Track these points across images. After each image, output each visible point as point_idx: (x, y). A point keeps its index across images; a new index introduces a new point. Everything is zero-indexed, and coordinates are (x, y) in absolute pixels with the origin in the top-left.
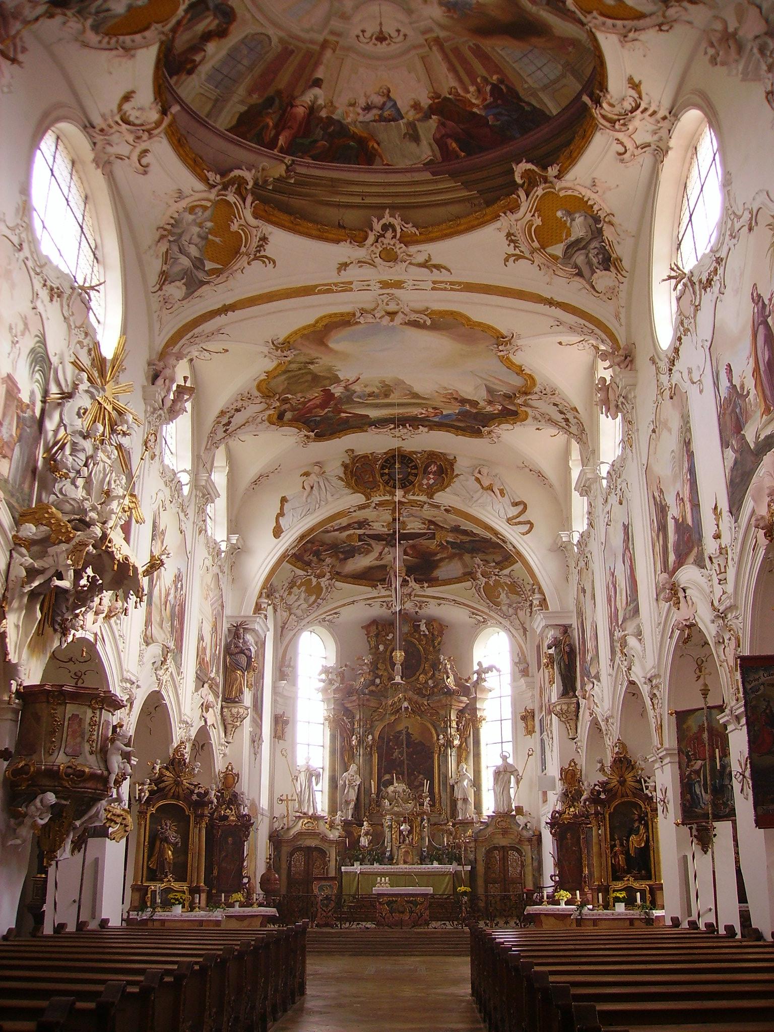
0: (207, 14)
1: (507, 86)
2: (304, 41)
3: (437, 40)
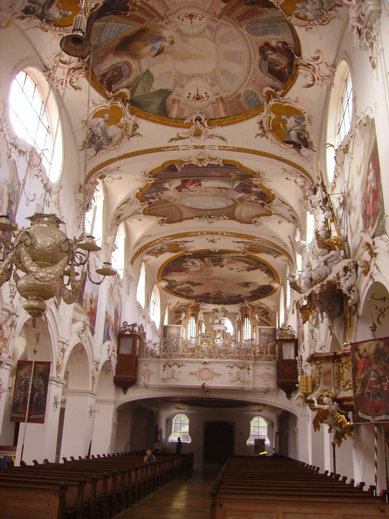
0: (270, 60)
1: (122, 14)
2: (230, 21)
3: (163, 19)
